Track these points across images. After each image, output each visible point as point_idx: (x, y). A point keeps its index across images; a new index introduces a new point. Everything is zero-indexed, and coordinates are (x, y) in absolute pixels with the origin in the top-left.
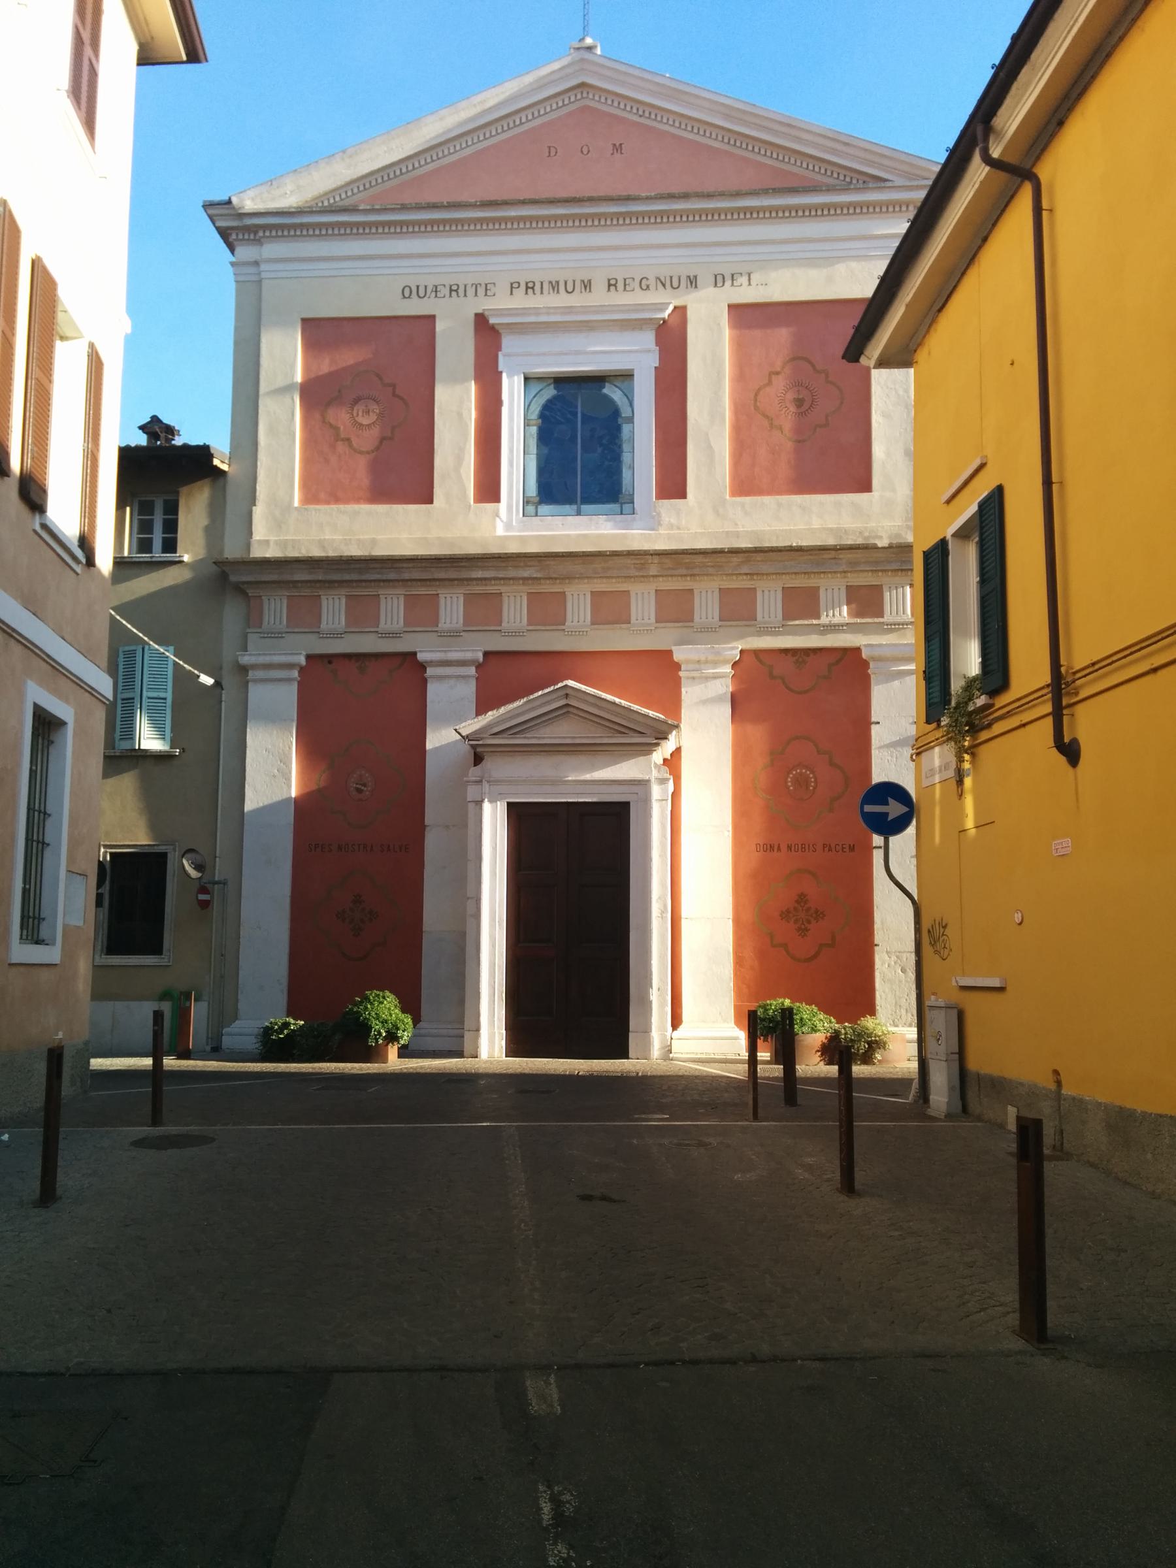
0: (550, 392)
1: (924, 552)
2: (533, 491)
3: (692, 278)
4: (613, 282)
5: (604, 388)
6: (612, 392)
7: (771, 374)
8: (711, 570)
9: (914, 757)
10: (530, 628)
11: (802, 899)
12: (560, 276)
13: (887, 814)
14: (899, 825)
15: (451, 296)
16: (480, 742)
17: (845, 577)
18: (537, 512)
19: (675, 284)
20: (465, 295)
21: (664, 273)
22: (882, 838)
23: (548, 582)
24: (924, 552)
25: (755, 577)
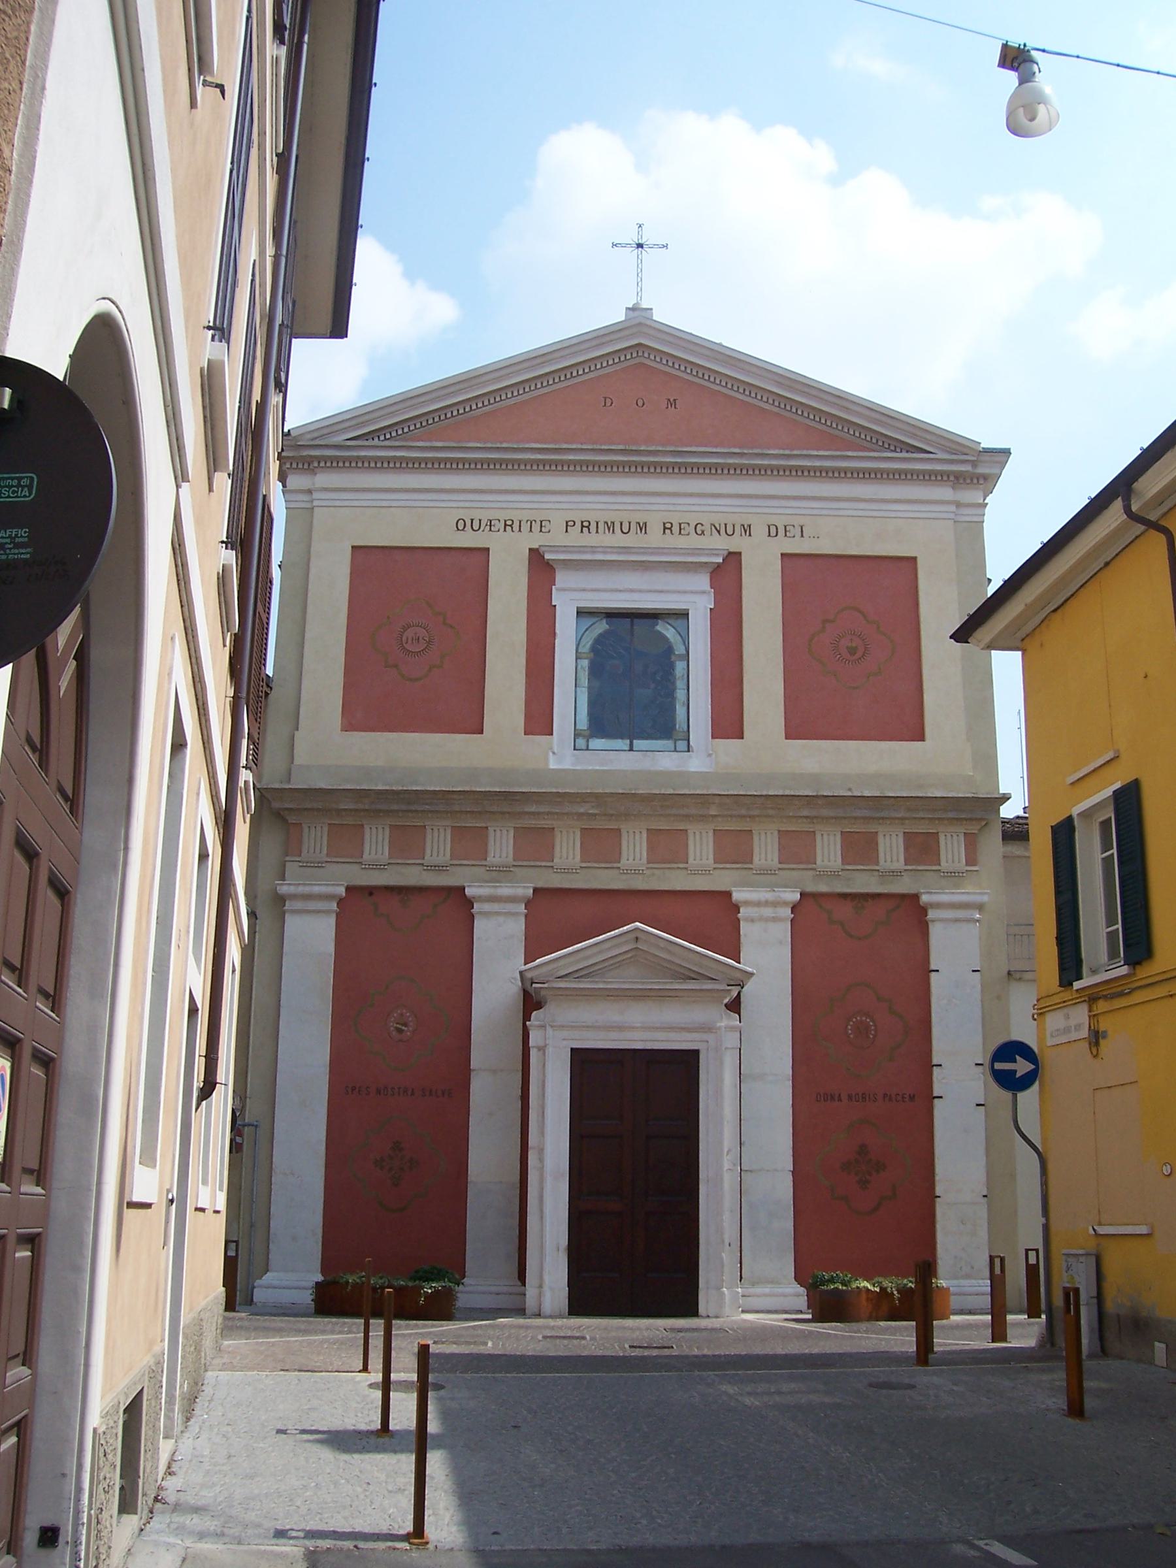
0: (602, 626)
1: (1052, 827)
2: (583, 724)
3: (746, 526)
4: (668, 525)
5: (657, 625)
6: (667, 631)
7: (825, 621)
8: (771, 812)
9: (1035, 1016)
10: (584, 865)
11: (863, 1149)
12: (616, 517)
13: (1015, 1071)
14: (1025, 1082)
15: (505, 530)
16: (546, 985)
17: (903, 824)
18: (588, 746)
19: (730, 531)
20: (520, 530)
21: (718, 520)
22: (1011, 1094)
23: (603, 818)
24: (1052, 827)
25: (815, 821)
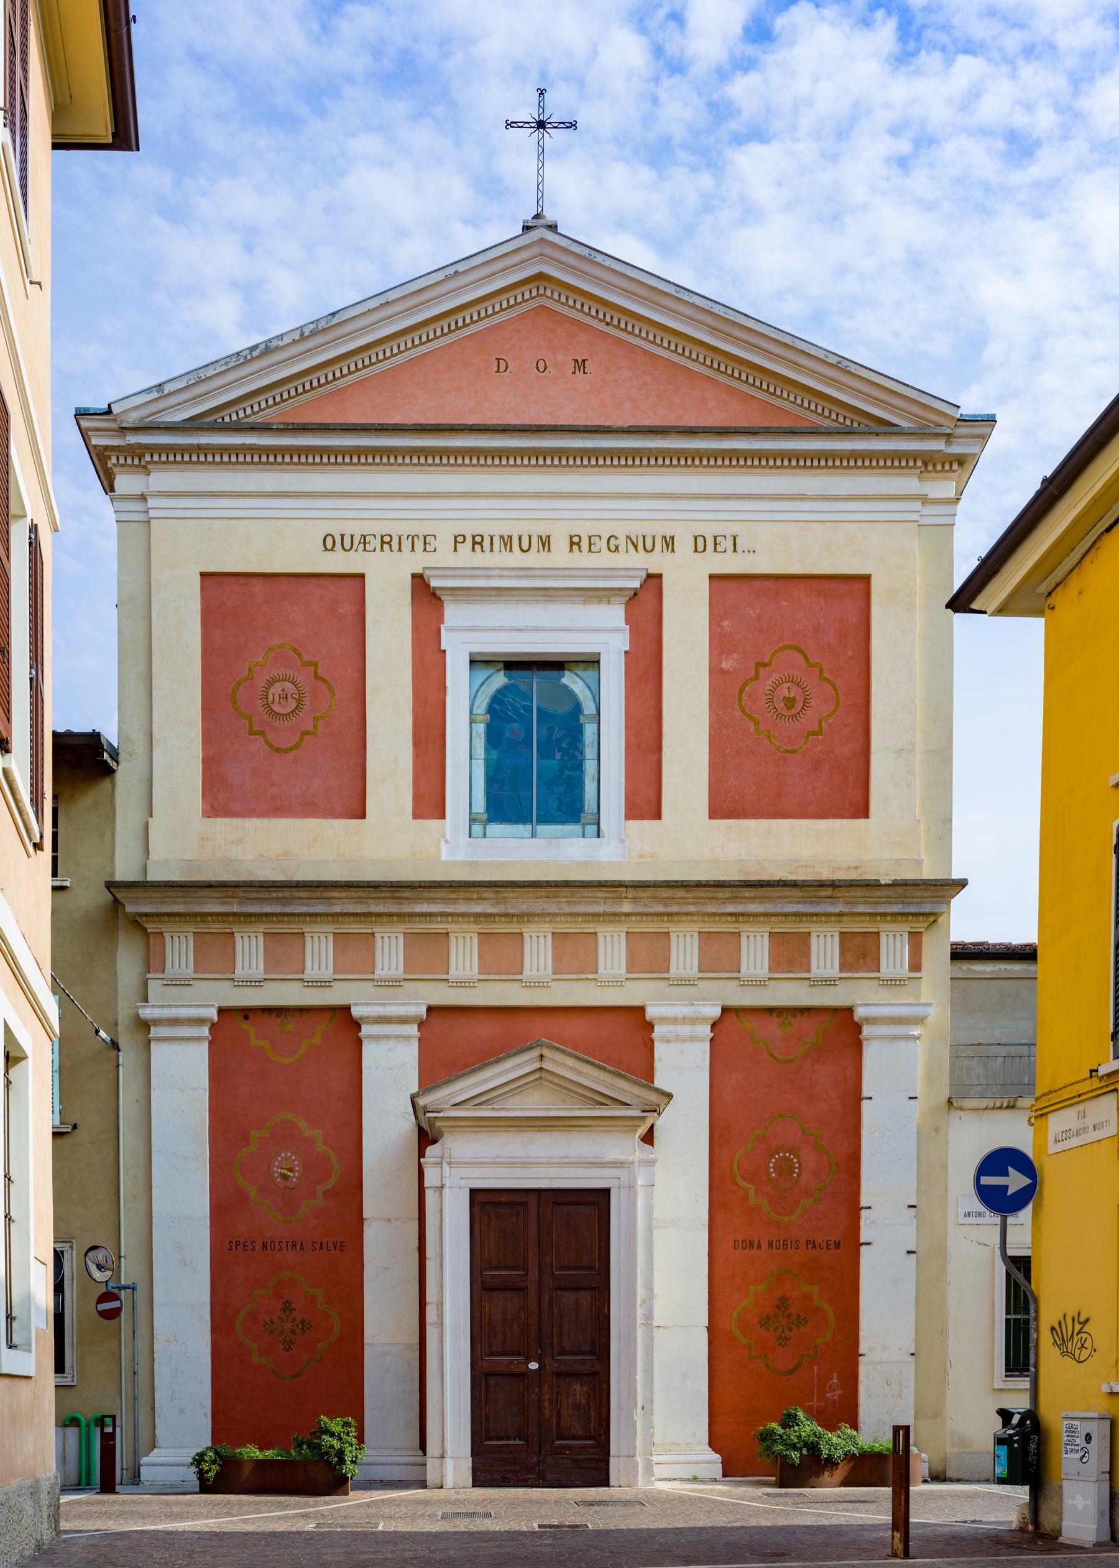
2: (480, 806)
4: (576, 540)
5: (564, 676)
7: (760, 665)
19: (649, 546)
20: (400, 550)
21: (636, 530)
